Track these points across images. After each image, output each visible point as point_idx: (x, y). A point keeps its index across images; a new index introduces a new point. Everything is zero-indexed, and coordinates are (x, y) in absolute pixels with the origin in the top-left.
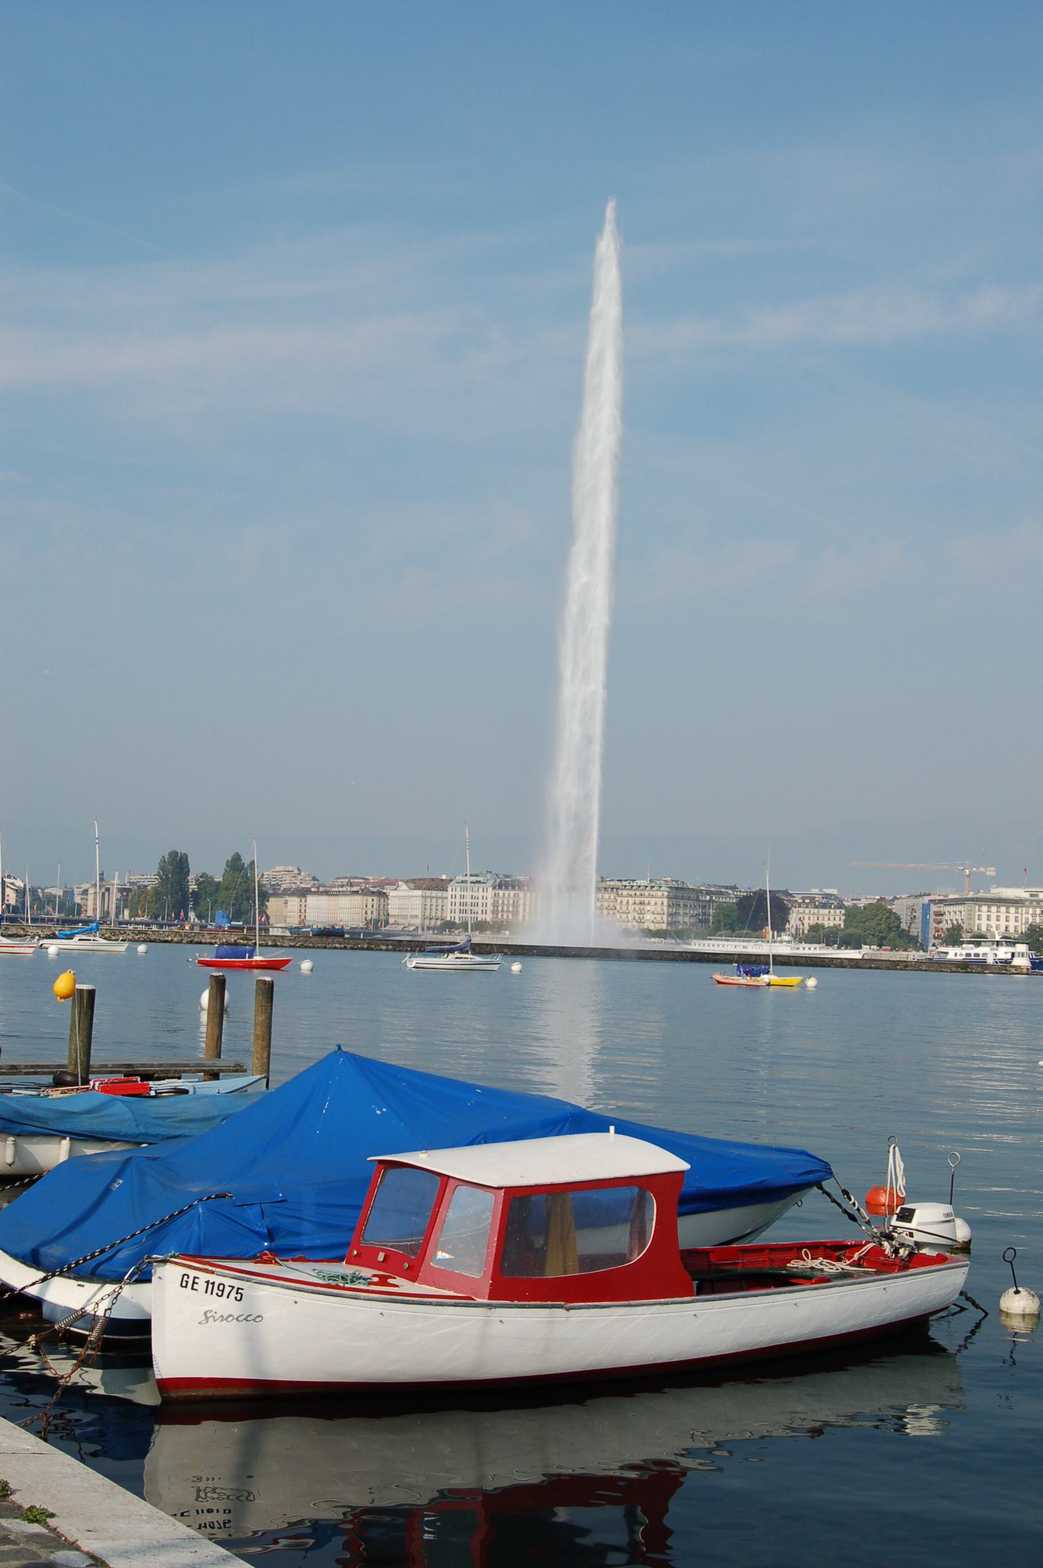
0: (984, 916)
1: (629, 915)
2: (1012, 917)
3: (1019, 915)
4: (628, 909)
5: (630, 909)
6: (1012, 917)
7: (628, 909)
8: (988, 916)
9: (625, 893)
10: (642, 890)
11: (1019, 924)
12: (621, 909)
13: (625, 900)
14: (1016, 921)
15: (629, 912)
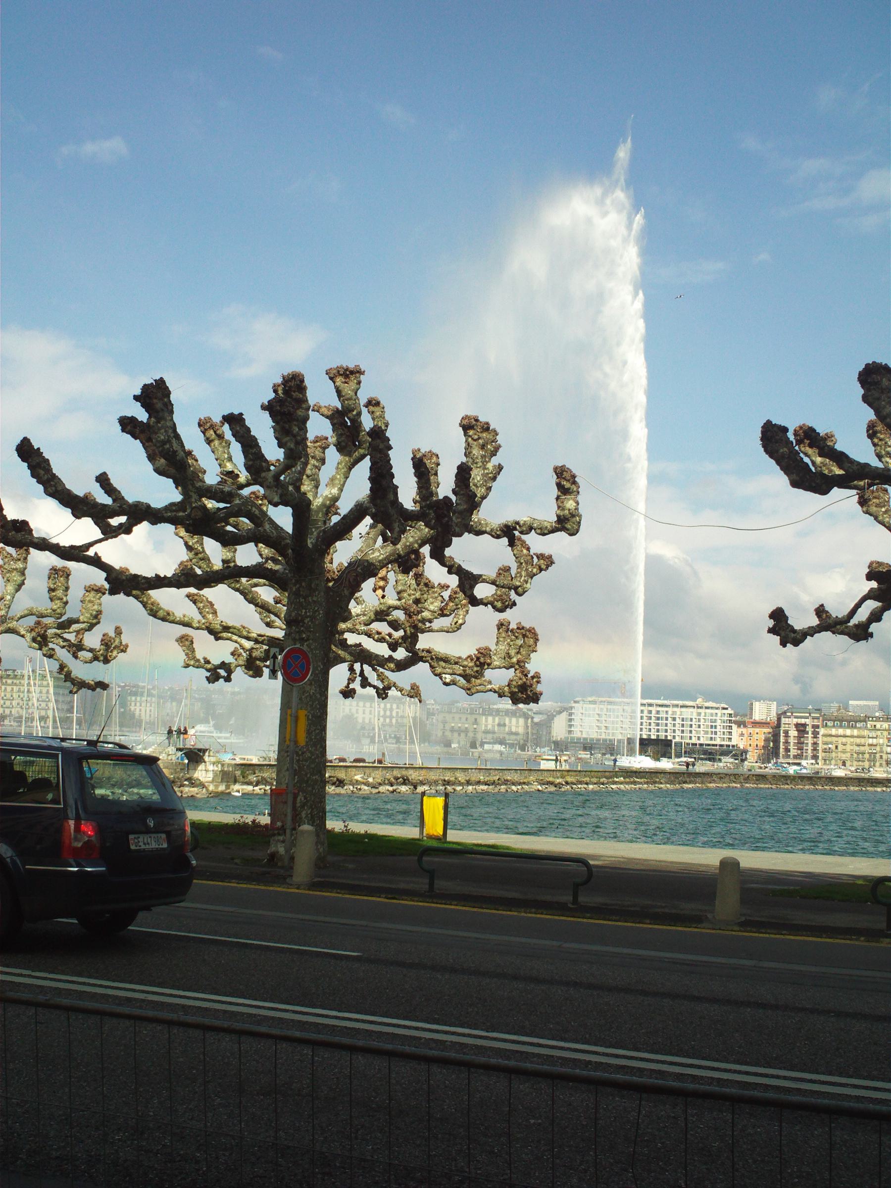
0: (361, 710)
1: (14, 702)
2: (367, 710)
3: (373, 709)
4: (12, 696)
5: (14, 696)
6: (367, 710)
7: (12, 696)
8: (364, 711)
9: (9, 681)
10: (20, 679)
11: (372, 716)
12: (5, 696)
13: (9, 688)
14: (370, 714)
15: (13, 700)
